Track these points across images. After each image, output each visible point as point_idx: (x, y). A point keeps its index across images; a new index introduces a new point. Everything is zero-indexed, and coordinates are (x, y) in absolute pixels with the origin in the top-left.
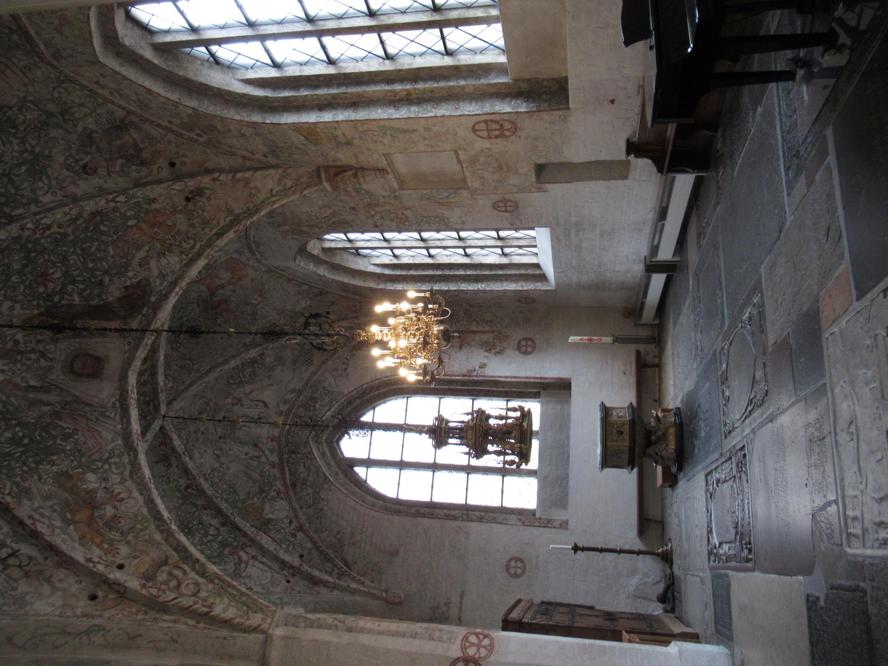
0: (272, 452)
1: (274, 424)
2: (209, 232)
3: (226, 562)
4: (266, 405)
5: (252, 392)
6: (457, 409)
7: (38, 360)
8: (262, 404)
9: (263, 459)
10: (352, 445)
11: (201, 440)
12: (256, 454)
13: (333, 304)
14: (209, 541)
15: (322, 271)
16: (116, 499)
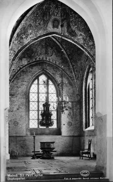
0: (39, 58)
2: (89, 50)
6: (53, 107)
7: (56, 13)
9: (37, 56)
10: (43, 78)
16: (27, 37)
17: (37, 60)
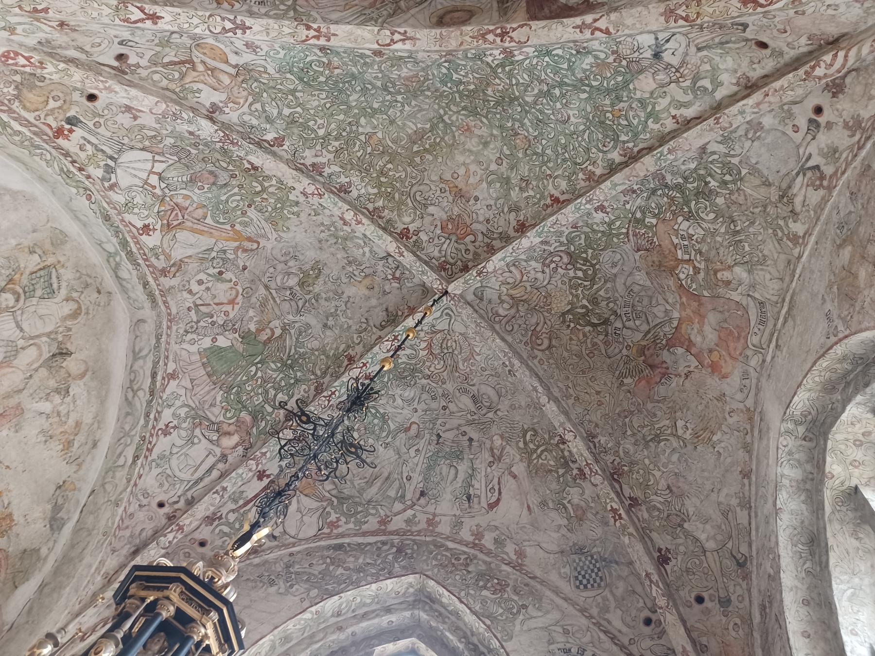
0: (408, 521)
1: (458, 524)
3: (227, 410)
4: (492, 506)
5: (515, 477)
8: (494, 499)
9: (398, 506)
11: (434, 405)
12: (409, 496)
13: (725, 602)
14: (267, 392)
15: (789, 511)
17: (391, 527)
